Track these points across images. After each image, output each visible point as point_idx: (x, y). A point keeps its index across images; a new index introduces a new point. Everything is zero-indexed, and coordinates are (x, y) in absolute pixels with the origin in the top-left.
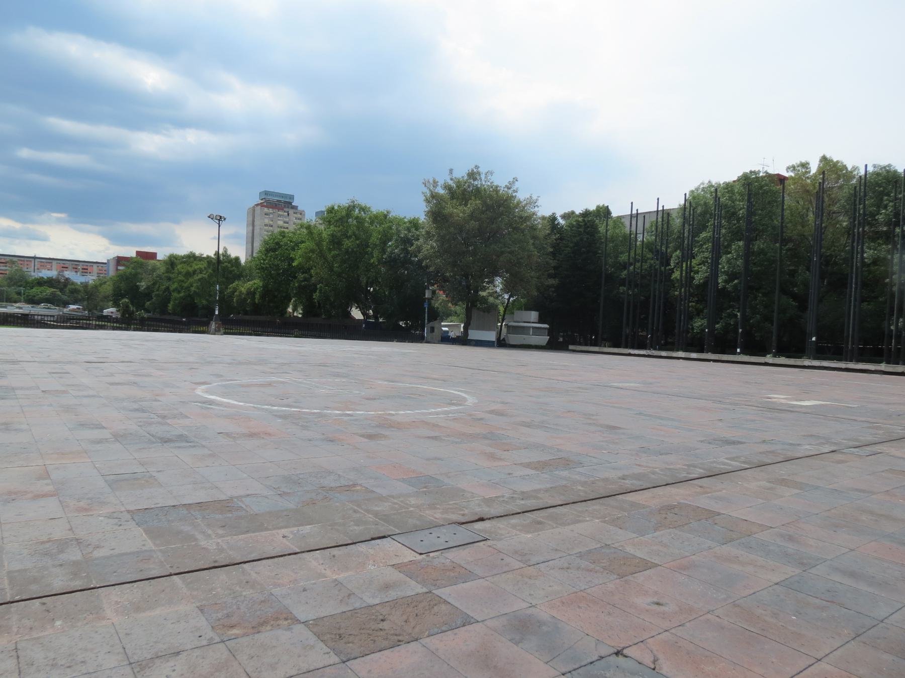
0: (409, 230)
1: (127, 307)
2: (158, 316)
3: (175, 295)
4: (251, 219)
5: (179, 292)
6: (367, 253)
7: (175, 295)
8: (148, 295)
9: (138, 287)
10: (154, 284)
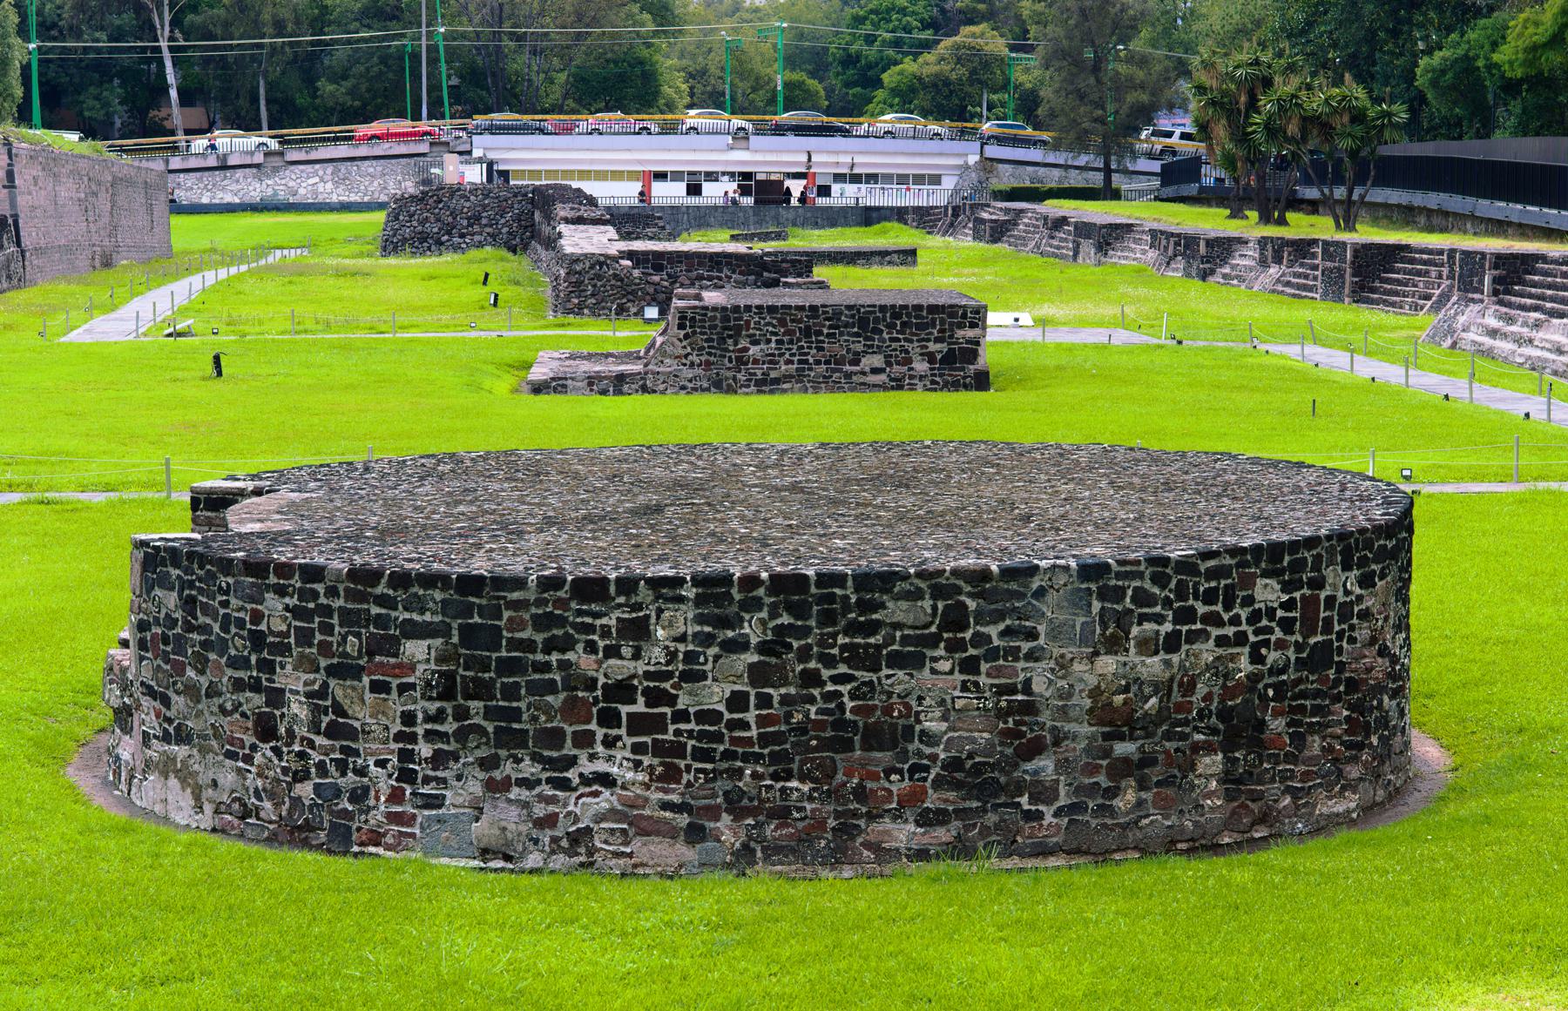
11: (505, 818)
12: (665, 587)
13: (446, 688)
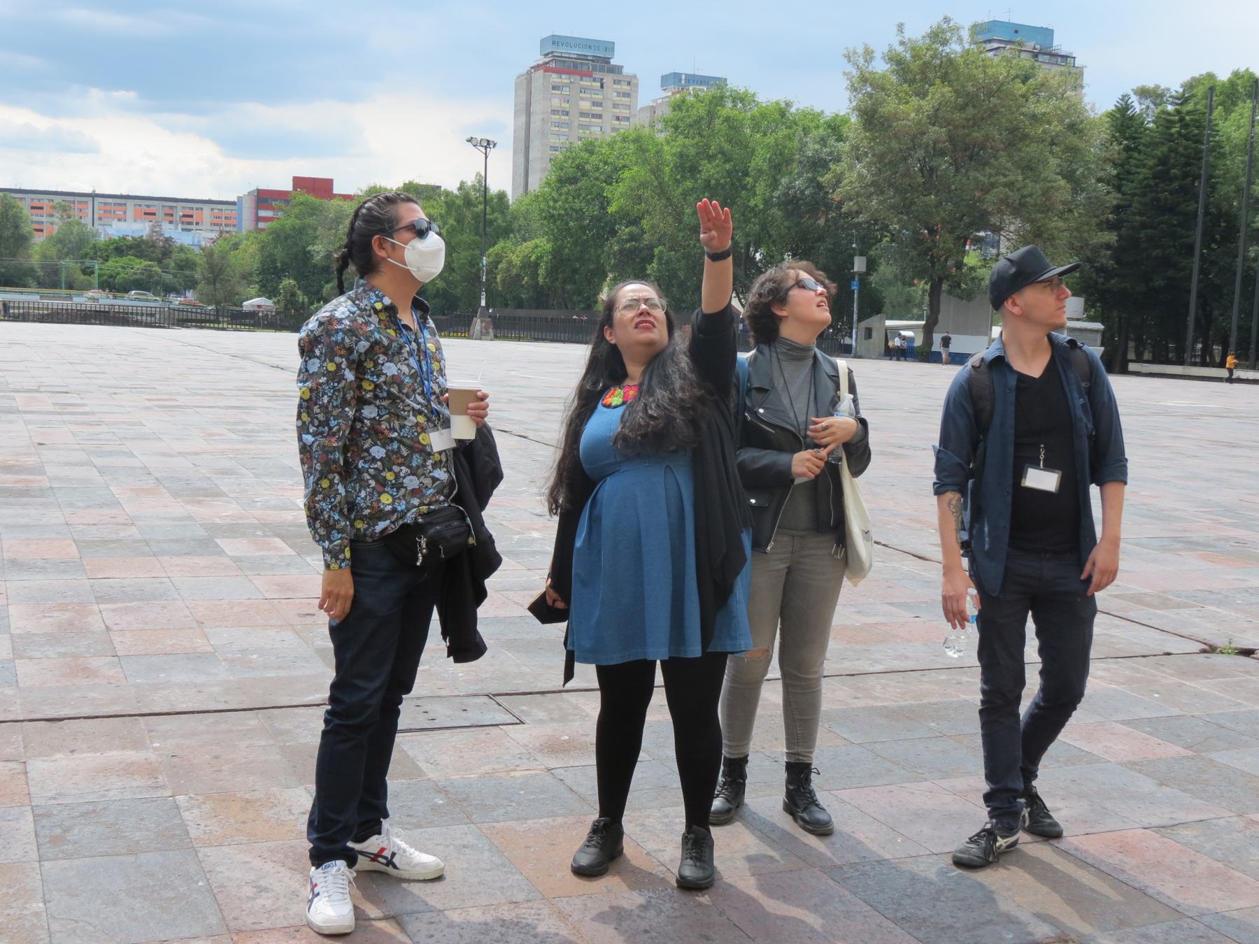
0: (823, 141)
1: (293, 295)
4: (524, 99)
6: (744, 187)
9: (307, 255)
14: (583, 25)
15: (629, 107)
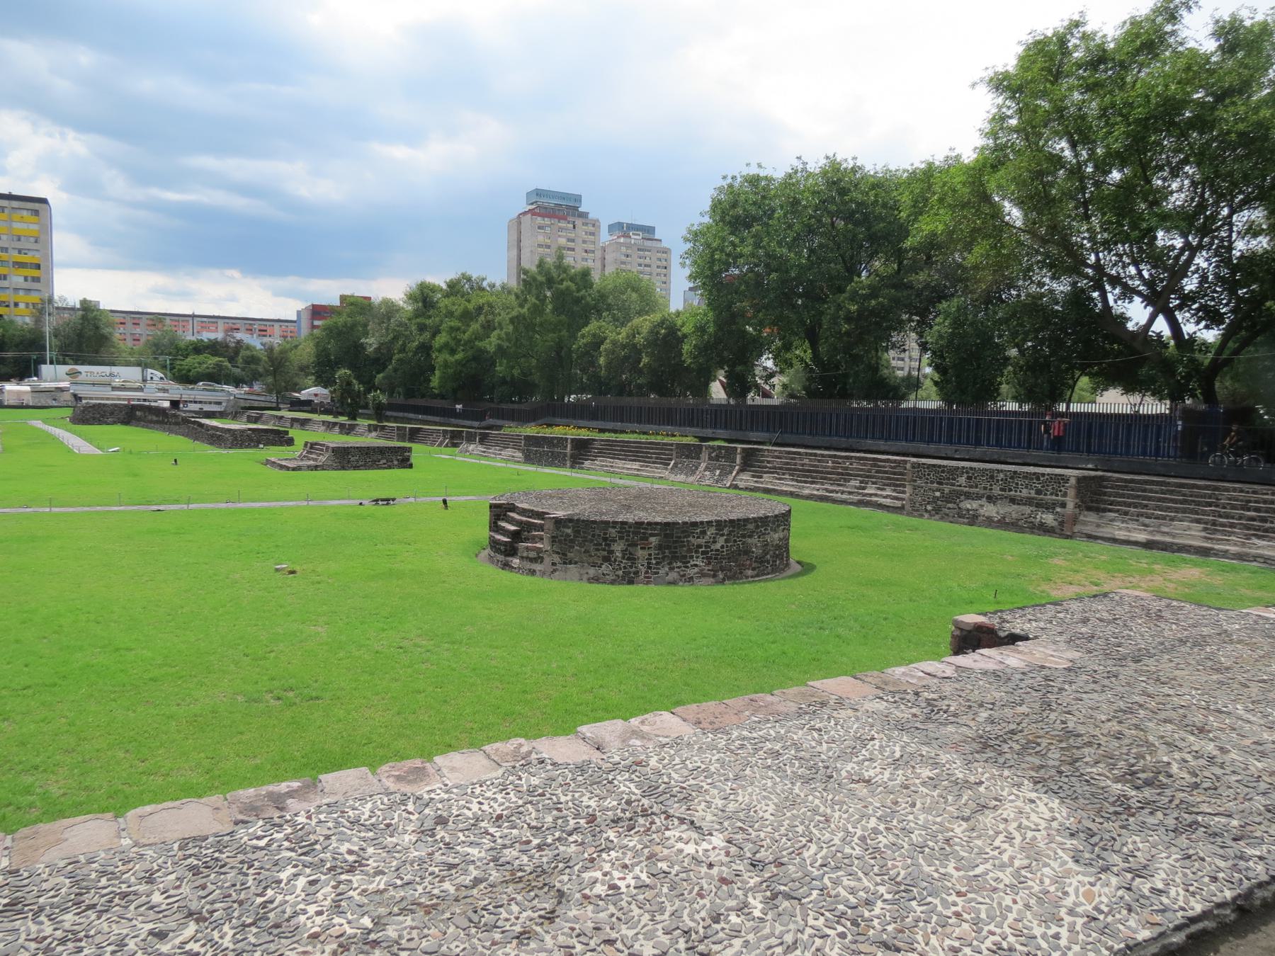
1: (349, 384)
2: (400, 400)
3: (440, 358)
4: (515, 237)
5: (453, 352)
7: (445, 356)
8: (380, 361)
9: (362, 347)
10: (395, 338)
11: (673, 575)
12: (709, 523)
13: (660, 547)
14: (558, 182)
15: (594, 243)
